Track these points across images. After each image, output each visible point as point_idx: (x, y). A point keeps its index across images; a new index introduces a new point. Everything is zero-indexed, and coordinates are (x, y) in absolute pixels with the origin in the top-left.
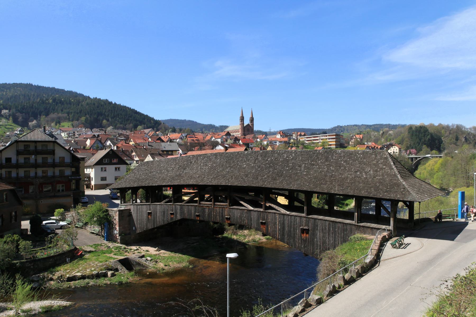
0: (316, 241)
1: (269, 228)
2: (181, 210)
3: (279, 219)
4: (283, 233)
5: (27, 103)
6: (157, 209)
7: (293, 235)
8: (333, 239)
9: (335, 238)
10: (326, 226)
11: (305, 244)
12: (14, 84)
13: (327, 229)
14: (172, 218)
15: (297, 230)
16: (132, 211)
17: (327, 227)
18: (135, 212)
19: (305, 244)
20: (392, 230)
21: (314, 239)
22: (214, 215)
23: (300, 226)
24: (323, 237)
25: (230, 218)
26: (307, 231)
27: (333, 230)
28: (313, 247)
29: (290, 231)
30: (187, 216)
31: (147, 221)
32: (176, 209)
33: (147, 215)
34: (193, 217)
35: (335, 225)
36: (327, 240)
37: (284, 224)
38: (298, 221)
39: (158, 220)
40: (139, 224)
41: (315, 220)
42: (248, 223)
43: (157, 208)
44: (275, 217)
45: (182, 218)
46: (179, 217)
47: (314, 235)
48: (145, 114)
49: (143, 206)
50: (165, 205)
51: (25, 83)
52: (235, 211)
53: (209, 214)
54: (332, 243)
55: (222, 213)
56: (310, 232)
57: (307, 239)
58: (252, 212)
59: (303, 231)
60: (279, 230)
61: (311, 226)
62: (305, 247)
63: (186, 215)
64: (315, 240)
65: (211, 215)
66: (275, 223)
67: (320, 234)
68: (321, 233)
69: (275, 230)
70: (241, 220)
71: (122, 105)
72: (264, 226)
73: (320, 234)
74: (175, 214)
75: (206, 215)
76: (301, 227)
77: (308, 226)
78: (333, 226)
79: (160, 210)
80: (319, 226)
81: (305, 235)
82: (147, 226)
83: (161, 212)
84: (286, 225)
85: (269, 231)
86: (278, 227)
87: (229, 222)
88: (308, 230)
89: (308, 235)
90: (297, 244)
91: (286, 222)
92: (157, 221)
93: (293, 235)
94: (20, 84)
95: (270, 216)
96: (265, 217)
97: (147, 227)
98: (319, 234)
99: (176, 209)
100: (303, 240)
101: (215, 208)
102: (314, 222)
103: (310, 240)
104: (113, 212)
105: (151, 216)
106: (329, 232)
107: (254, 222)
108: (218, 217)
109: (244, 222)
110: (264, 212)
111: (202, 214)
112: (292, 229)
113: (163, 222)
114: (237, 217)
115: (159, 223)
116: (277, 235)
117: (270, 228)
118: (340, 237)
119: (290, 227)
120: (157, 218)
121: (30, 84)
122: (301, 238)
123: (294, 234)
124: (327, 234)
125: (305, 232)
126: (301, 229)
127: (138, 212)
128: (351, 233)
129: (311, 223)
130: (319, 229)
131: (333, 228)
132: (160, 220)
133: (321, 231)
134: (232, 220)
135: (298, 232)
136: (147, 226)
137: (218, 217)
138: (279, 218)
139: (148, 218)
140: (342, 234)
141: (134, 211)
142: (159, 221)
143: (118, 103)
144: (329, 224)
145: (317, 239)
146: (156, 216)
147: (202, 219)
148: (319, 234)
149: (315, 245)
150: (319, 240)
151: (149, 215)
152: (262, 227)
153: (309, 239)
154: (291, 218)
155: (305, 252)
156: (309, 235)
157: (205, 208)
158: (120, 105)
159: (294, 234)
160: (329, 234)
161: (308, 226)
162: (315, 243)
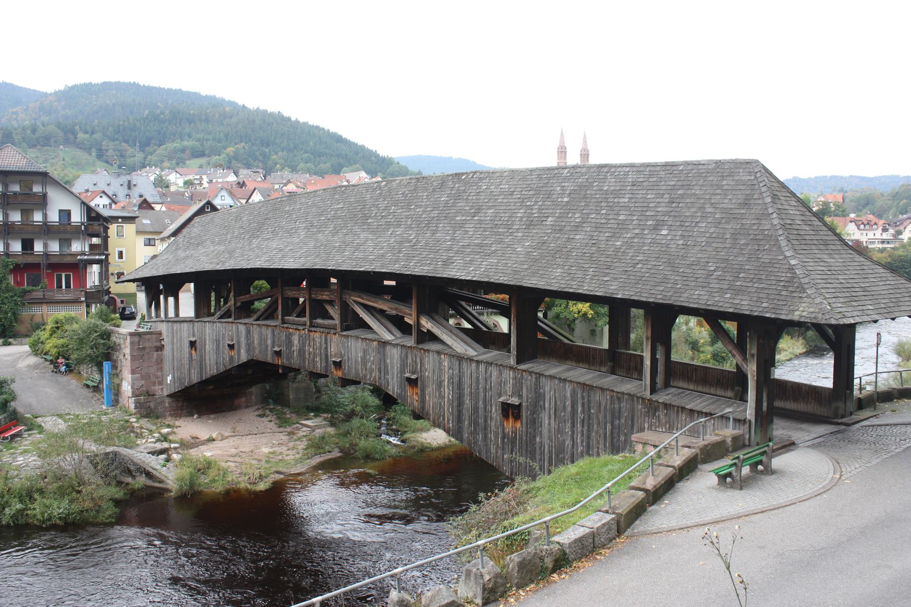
2: (247, 337)
4: (460, 412)
5: (124, 121)
6: (205, 335)
8: (582, 442)
9: (589, 437)
10: (565, 397)
12: (105, 83)
13: (569, 409)
14: (231, 358)
16: (164, 336)
17: (568, 403)
20: (750, 421)
21: (535, 437)
22: (310, 354)
23: (500, 395)
24: (559, 431)
25: (341, 361)
27: (583, 412)
29: (476, 409)
30: (258, 355)
32: (238, 336)
34: (269, 359)
35: (589, 396)
36: (568, 442)
37: (460, 385)
38: (494, 378)
40: (177, 369)
42: (380, 378)
45: (250, 358)
46: (244, 357)
47: (534, 423)
48: (360, 143)
51: (127, 80)
55: (326, 348)
57: (516, 434)
59: (510, 411)
60: (451, 402)
61: (527, 396)
63: (257, 351)
64: (538, 439)
66: (440, 385)
69: (440, 404)
70: (366, 369)
71: (311, 123)
75: (293, 351)
76: (501, 400)
77: (520, 396)
78: (583, 398)
79: (211, 337)
80: (547, 397)
81: (511, 420)
84: (467, 391)
87: (340, 374)
89: (518, 425)
91: (467, 380)
92: (205, 363)
94: (116, 83)
97: (190, 379)
98: (547, 422)
99: (238, 336)
100: (508, 439)
101: (312, 334)
105: (195, 350)
107: (393, 378)
108: (318, 359)
111: (286, 349)
112: (481, 402)
113: (217, 369)
116: (444, 419)
117: (430, 397)
118: (602, 436)
119: (475, 397)
120: (205, 355)
121: (134, 83)
122: (503, 432)
124: (569, 425)
126: (503, 403)
127: (175, 341)
130: (547, 405)
131: (583, 406)
133: (552, 412)
134: (345, 366)
135: (495, 412)
137: (318, 359)
138: (449, 369)
140: (609, 426)
143: (301, 120)
144: (574, 394)
145: (541, 437)
147: (286, 362)
150: (546, 442)
151: (192, 349)
152: (409, 391)
154: (478, 368)
156: (522, 424)
157: (291, 334)
158: (305, 124)
160: (573, 425)
161: (520, 396)
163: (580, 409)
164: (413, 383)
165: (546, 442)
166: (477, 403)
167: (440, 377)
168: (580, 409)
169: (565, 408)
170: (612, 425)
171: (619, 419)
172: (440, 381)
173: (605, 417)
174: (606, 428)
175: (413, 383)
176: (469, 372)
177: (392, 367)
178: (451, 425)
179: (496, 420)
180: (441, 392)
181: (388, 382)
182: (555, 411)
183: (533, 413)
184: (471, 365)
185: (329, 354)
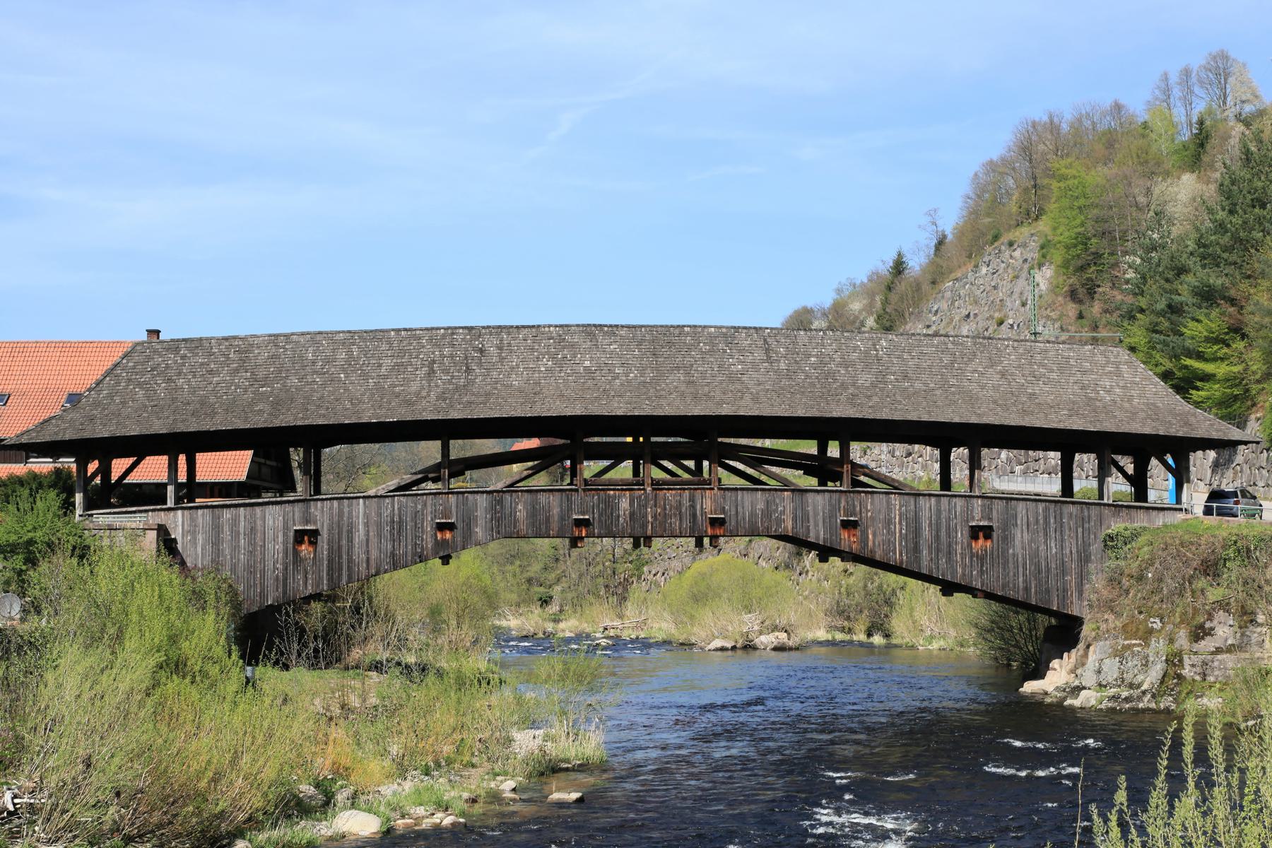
0: (1014, 555)
1: (870, 537)
3: (900, 509)
7: (944, 547)
8: (1056, 545)
9: (1062, 540)
11: (982, 566)
13: (1041, 522)
15: (956, 533)
18: (200, 537)
19: (982, 566)
22: (655, 517)
24: (1030, 542)
26: (987, 532)
28: (1004, 569)
31: (286, 569)
33: (285, 543)
35: (1061, 509)
36: (1042, 547)
37: (917, 518)
38: (958, 509)
39: (359, 554)
41: (1007, 503)
43: (350, 513)
44: (888, 503)
47: (1007, 539)
49: (258, 510)
50: (402, 498)
52: (743, 498)
53: (632, 514)
54: (1056, 553)
56: (995, 535)
57: (986, 551)
58: (810, 496)
59: (975, 532)
62: (982, 572)
64: (1011, 551)
65: (645, 516)
66: (888, 522)
67: (1022, 537)
68: (1025, 534)
69: (889, 540)
72: (853, 532)
73: (1022, 537)
74: (460, 525)
75: (619, 517)
77: (990, 519)
78: (1055, 512)
80: (1019, 516)
81: (981, 541)
82: (285, 585)
83: (379, 525)
84: (925, 525)
85: (870, 543)
86: (899, 528)
88: (990, 528)
89: (989, 543)
90: (960, 570)
91: (925, 515)
92: (350, 561)
93: (944, 547)
95: (872, 504)
96: (854, 506)
97: (285, 592)
98: (1020, 536)
101: (661, 493)
102: (1007, 507)
103: (995, 553)
104: (120, 533)
106: (1045, 530)
107: (816, 525)
109: (779, 525)
110: (850, 492)
111: (600, 515)
114: (753, 514)
115: (368, 568)
116: (895, 553)
117: (874, 535)
123: (950, 545)
124: (1041, 534)
125: (981, 535)
126: (972, 527)
128: (1101, 526)
129: (998, 511)
130: (1019, 522)
131: (1055, 518)
132: (374, 554)
135: (961, 535)
136: (285, 585)
138: (901, 506)
139: (296, 553)
140: (1080, 530)
141: (194, 533)
142: (368, 560)
144: (1046, 510)
145: (1014, 550)
146: (350, 540)
148: (1020, 537)
149: (1011, 565)
150: (1019, 550)
152: (844, 535)
153: (992, 553)
154: (938, 503)
155: (982, 586)
156: (992, 541)
159: (950, 545)
162: (1011, 559)
163: (1052, 521)
164: (847, 525)
165: (1019, 550)
166: (938, 530)
167: (888, 515)
168: (1052, 521)
169: (1037, 522)
170: (1083, 528)
171: (1089, 523)
172: (889, 520)
173: (1076, 523)
174: (1077, 532)
175: (847, 525)
176: (928, 505)
177: (816, 515)
178: (905, 558)
179: (962, 543)
180: (890, 528)
181: (809, 530)
182: (1028, 525)
183: (1004, 531)
184: (930, 500)
185: (698, 513)
